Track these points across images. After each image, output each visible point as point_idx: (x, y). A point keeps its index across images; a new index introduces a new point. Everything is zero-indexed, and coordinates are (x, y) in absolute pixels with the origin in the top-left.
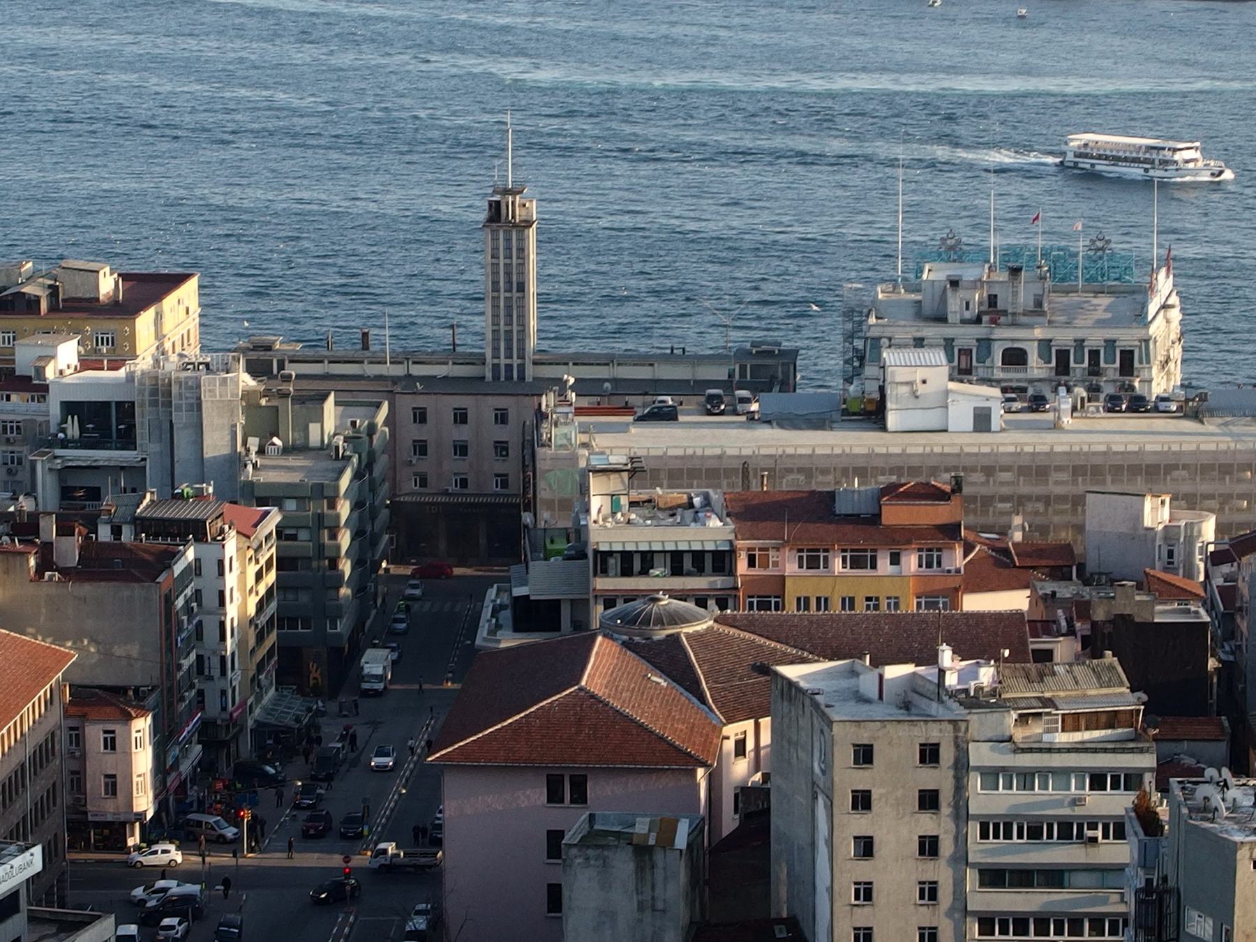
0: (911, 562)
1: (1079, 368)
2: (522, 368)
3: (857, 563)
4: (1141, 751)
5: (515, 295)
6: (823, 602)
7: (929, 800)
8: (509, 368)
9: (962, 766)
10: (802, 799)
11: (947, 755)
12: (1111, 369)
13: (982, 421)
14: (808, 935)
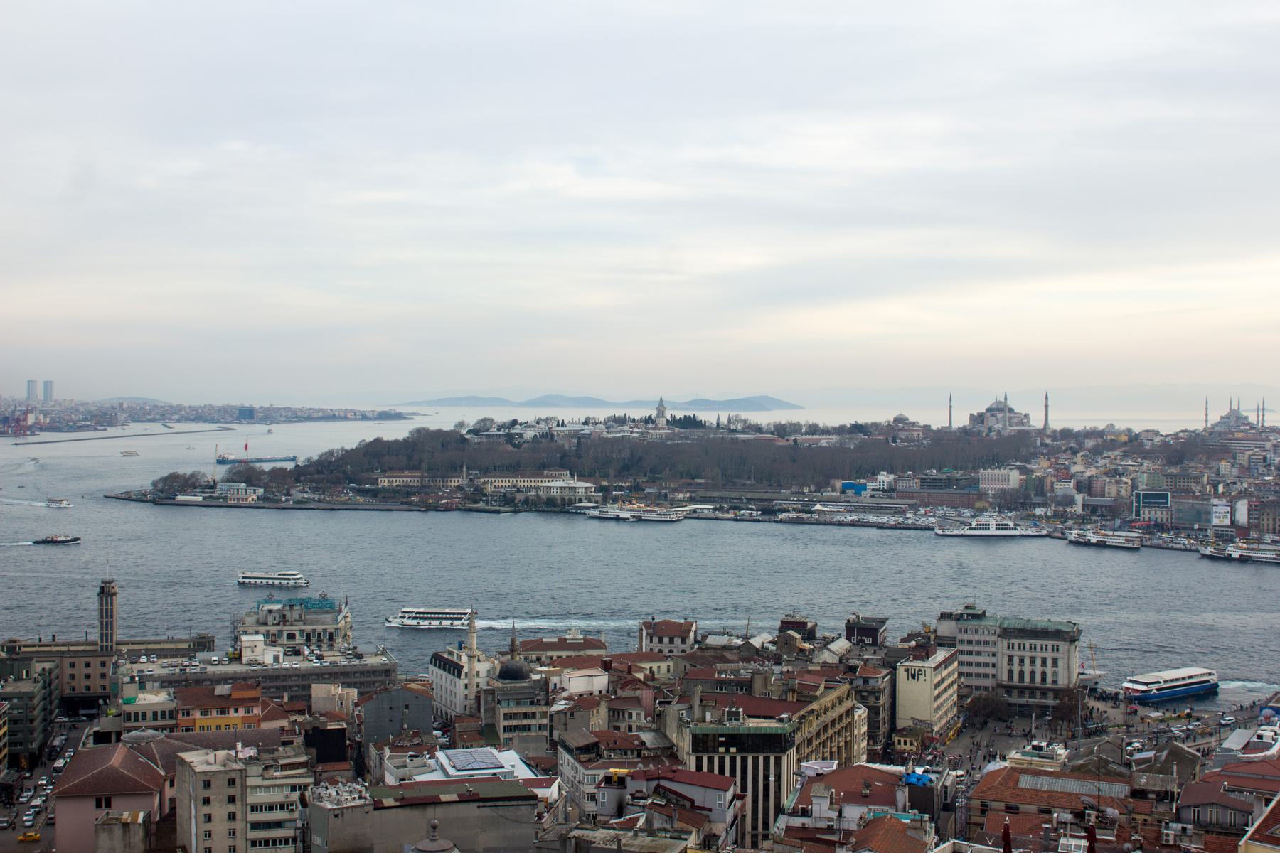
0: (241, 712)
1: (314, 640)
2: (112, 646)
3: (223, 712)
4: (309, 777)
5: (109, 620)
6: (209, 728)
7: (232, 799)
8: (107, 646)
9: (244, 787)
10: (187, 802)
11: (238, 782)
12: (326, 639)
13: (276, 658)
14: (189, 851)
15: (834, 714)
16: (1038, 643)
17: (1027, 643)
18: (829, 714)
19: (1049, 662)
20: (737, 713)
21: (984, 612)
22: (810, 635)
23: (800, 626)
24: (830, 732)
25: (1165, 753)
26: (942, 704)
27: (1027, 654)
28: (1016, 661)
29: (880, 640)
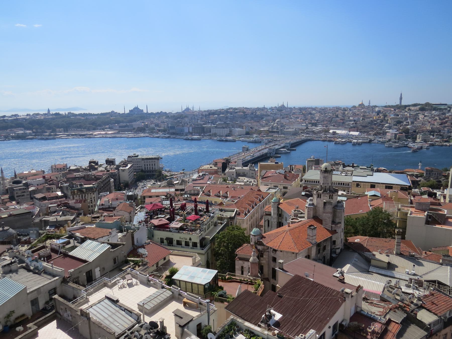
15: (106, 182)
16: (151, 161)
17: (148, 161)
18: (104, 182)
19: (153, 165)
20: (82, 184)
21: (138, 155)
22: (97, 163)
23: (94, 162)
24: (105, 186)
25: (181, 181)
26: (130, 177)
27: (148, 163)
28: (146, 165)
29: (114, 163)
